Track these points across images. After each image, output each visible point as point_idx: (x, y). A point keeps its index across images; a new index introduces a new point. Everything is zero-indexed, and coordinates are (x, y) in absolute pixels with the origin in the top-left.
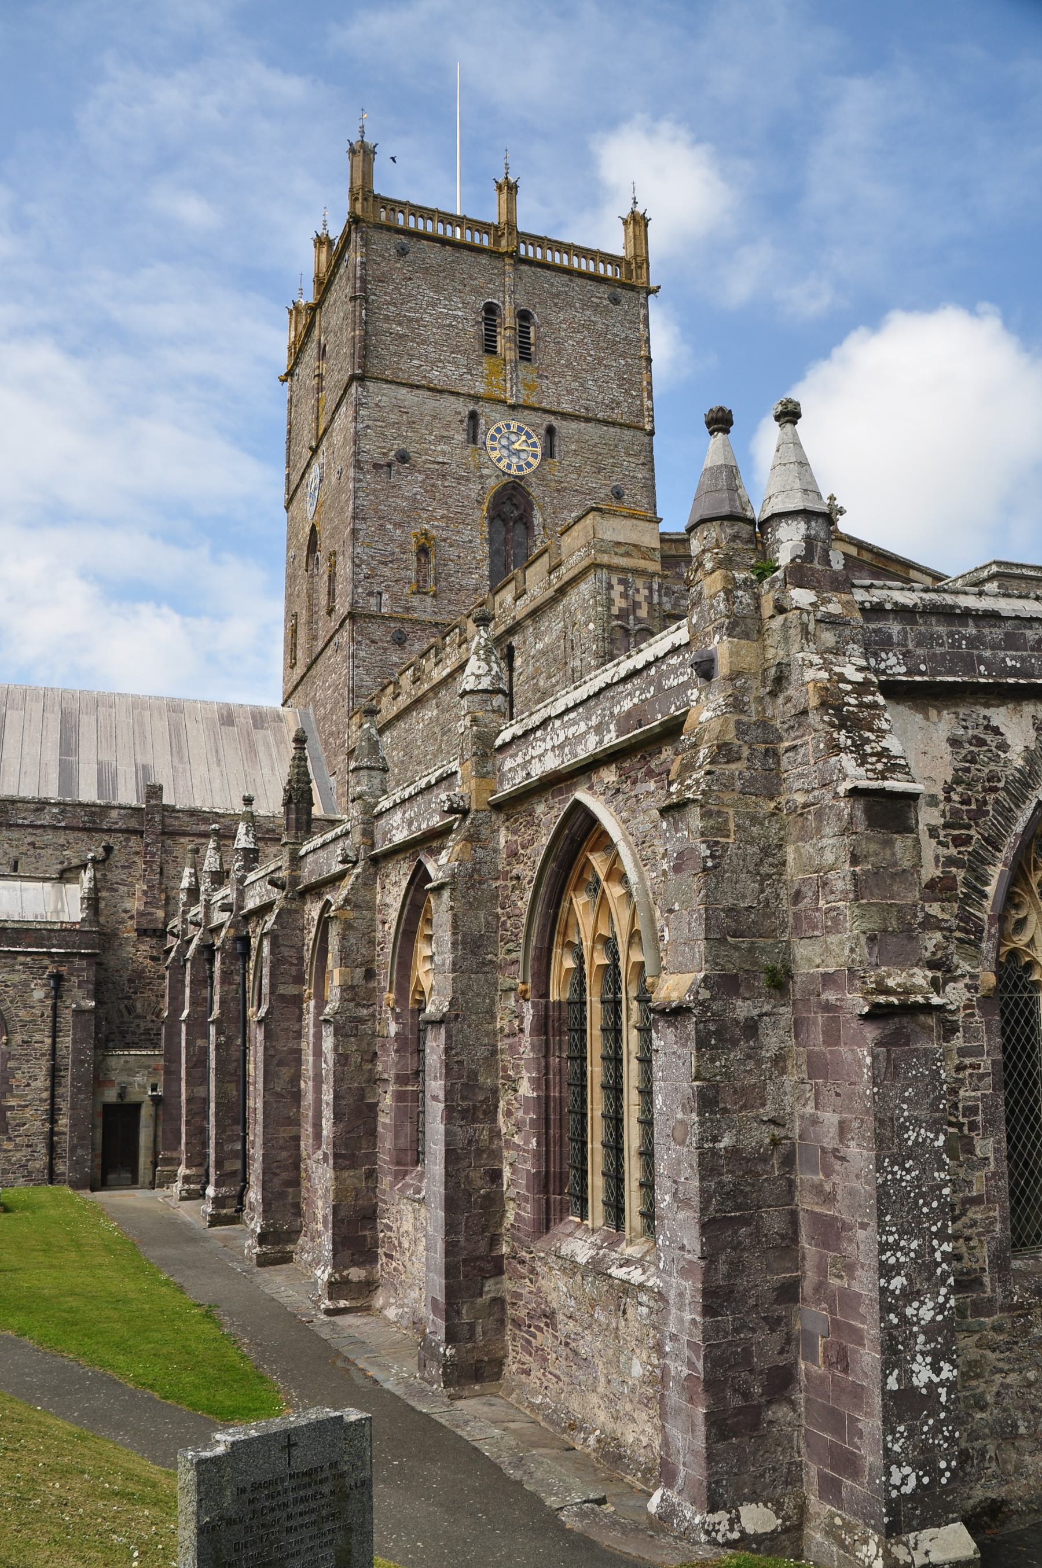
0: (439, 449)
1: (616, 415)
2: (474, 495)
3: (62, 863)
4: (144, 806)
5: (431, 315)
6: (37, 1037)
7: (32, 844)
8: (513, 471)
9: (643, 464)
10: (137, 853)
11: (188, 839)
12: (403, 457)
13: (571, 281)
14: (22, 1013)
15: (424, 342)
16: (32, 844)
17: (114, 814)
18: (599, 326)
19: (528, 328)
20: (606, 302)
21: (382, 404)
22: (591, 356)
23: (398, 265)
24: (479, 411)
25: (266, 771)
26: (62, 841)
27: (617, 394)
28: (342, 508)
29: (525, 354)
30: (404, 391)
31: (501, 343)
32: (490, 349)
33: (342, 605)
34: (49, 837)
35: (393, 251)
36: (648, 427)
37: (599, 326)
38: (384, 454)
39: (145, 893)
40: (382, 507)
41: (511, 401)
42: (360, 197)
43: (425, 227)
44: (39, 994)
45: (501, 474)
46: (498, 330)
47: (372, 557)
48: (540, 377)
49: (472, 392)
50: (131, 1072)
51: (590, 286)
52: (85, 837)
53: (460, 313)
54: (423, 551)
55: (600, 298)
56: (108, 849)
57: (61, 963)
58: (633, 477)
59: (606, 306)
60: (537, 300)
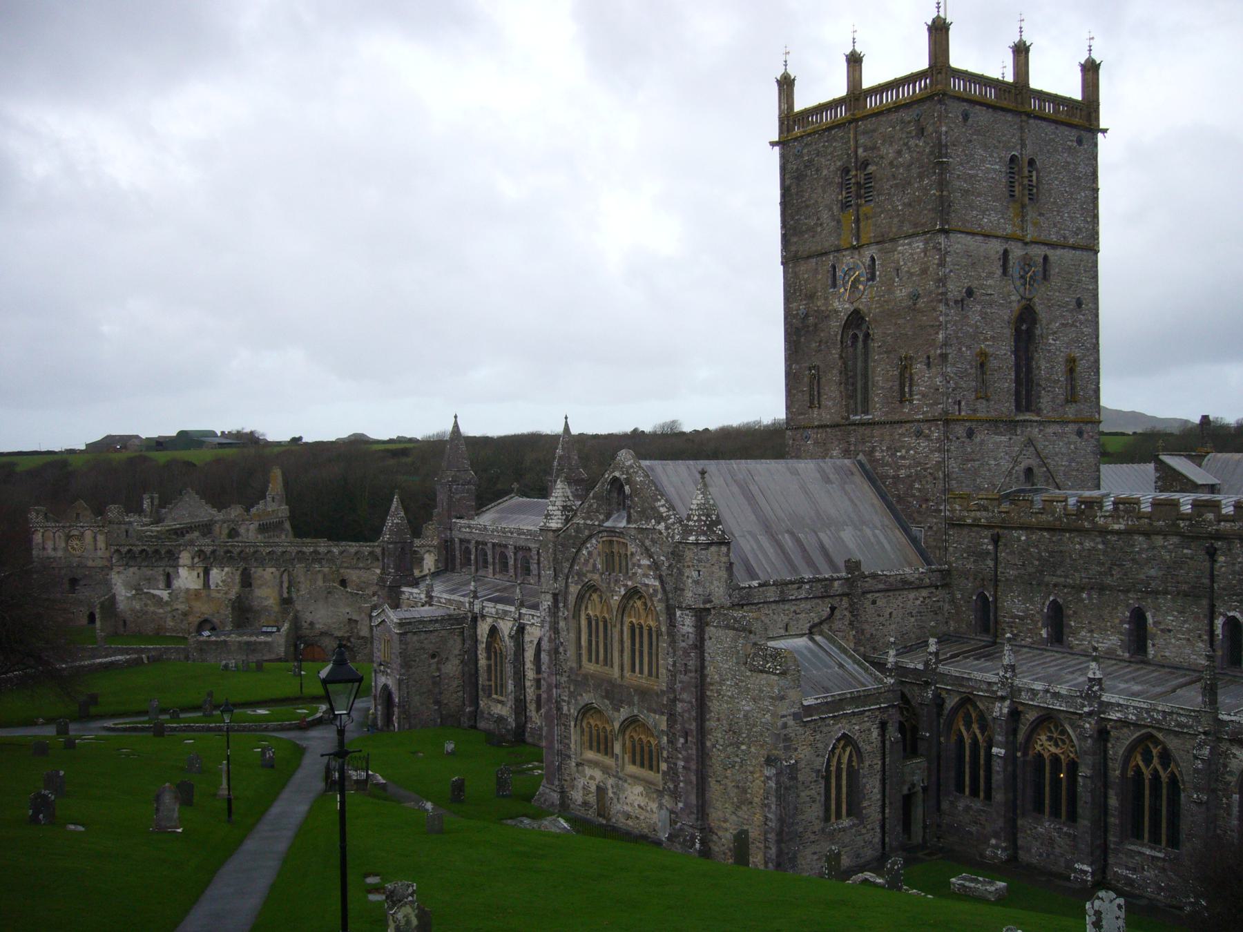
3: (810, 622)
6: (875, 762)
7: (795, 612)
9: (1093, 278)
10: (846, 609)
11: (871, 594)
12: (970, 292)
13: (1056, 128)
14: (868, 747)
15: (979, 195)
16: (795, 612)
17: (836, 584)
20: (1075, 144)
22: (1067, 192)
23: (964, 130)
26: (809, 607)
30: (969, 238)
31: (1017, 189)
34: (803, 605)
38: (959, 291)
39: (854, 636)
40: (960, 335)
41: (1028, 239)
44: (875, 733)
45: (1019, 298)
46: (1017, 177)
48: (1041, 214)
51: (1066, 131)
52: (820, 602)
53: (997, 167)
56: (833, 609)
57: (883, 713)
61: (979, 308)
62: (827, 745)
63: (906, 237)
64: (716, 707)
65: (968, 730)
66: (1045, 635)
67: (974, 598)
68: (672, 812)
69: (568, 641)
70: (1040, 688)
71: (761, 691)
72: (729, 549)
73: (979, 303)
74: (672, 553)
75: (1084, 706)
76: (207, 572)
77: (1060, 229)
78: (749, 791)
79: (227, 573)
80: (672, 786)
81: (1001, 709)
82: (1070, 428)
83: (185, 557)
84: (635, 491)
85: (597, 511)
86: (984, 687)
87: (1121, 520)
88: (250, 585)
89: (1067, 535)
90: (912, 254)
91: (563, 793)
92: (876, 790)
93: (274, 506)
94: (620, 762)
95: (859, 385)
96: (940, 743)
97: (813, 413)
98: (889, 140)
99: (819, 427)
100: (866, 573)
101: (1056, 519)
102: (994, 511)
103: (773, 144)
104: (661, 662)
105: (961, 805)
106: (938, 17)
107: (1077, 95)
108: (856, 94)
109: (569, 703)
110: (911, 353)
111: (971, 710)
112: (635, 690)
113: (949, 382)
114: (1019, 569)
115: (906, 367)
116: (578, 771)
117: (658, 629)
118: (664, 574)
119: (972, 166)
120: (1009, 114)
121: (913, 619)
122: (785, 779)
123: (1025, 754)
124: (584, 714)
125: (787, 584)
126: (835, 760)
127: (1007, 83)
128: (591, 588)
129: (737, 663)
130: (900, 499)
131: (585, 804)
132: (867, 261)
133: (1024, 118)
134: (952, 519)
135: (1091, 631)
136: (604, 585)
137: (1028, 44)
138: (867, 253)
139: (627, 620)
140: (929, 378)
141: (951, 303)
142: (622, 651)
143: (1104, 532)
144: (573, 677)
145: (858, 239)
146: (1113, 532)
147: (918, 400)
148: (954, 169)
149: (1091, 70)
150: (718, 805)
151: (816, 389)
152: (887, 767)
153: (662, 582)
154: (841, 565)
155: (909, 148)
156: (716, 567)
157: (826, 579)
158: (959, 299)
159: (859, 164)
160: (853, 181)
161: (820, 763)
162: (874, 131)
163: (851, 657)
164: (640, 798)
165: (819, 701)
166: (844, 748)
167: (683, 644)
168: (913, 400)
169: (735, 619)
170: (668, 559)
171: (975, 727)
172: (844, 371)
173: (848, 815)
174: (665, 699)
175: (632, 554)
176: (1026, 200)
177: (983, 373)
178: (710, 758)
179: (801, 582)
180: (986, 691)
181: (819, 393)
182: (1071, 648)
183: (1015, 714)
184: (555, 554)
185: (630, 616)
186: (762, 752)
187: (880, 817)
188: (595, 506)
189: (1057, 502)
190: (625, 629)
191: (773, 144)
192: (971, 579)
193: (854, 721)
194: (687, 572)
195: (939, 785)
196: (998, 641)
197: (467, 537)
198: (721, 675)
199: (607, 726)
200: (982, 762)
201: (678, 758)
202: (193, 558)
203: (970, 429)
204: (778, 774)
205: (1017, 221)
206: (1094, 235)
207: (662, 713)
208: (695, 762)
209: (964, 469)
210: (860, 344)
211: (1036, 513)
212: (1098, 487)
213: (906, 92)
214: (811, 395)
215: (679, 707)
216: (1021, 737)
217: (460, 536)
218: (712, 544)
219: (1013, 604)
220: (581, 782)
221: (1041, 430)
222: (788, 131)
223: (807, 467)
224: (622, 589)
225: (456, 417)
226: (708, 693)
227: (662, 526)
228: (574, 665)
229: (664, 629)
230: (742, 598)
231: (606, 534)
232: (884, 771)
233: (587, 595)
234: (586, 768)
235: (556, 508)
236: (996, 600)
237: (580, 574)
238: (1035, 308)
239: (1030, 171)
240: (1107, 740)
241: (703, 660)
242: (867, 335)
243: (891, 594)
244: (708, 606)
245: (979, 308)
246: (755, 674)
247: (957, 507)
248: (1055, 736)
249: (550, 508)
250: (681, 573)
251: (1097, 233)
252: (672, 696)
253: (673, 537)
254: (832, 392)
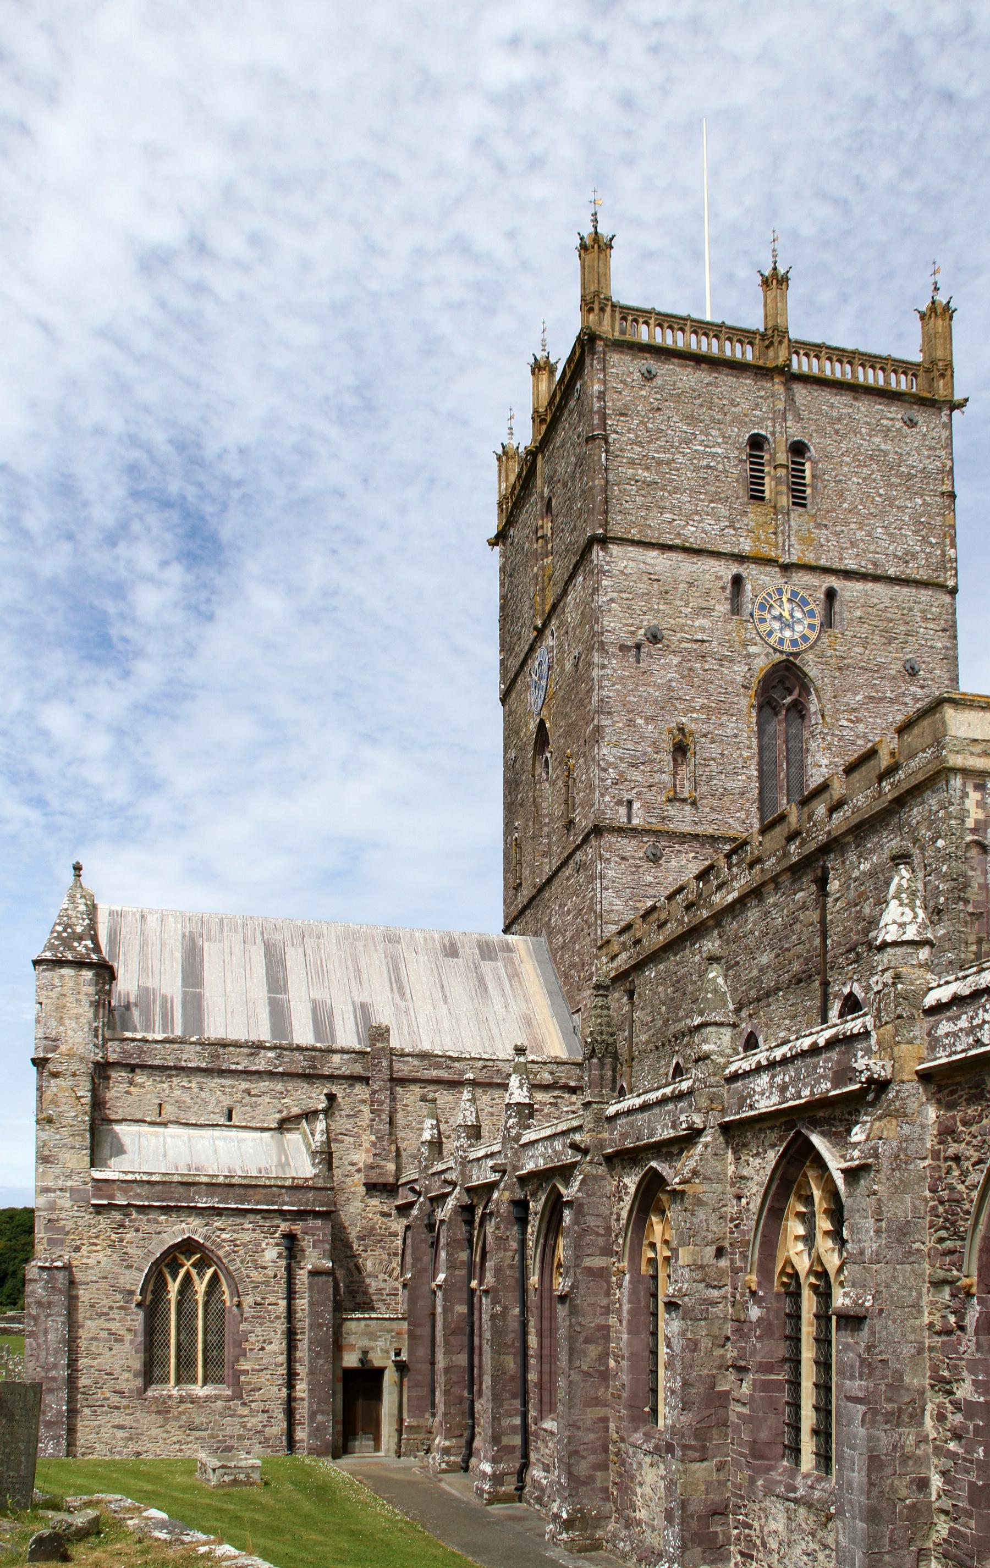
0: (697, 624)
1: (913, 570)
2: (739, 679)
4: (369, 1049)
5: (684, 455)
8: (786, 648)
9: (944, 630)
12: (655, 638)
15: (676, 490)
17: (336, 1058)
18: (891, 457)
19: (803, 464)
20: (899, 424)
21: (628, 571)
22: (880, 495)
24: (745, 575)
25: (499, 1007)
27: (913, 542)
28: (581, 701)
29: (799, 501)
30: (655, 553)
32: (757, 496)
33: (585, 817)
34: (265, 1085)
35: (637, 375)
36: (951, 583)
37: (891, 457)
38: (632, 633)
40: (632, 699)
41: (785, 559)
42: (596, 306)
43: (675, 341)
45: (771, 651)
46: (766, 469)
47: (621, 759)
48: (819, 526)
49: (736, 551)
53: (720, 451)
54: (680, 750)
55: (892, 419)
58: (932, 647)
59: (899, 430)
60: (814, 427)
61: (676, 660)
113: (605, 770)
238: (806, 669)
245: (676, 660)
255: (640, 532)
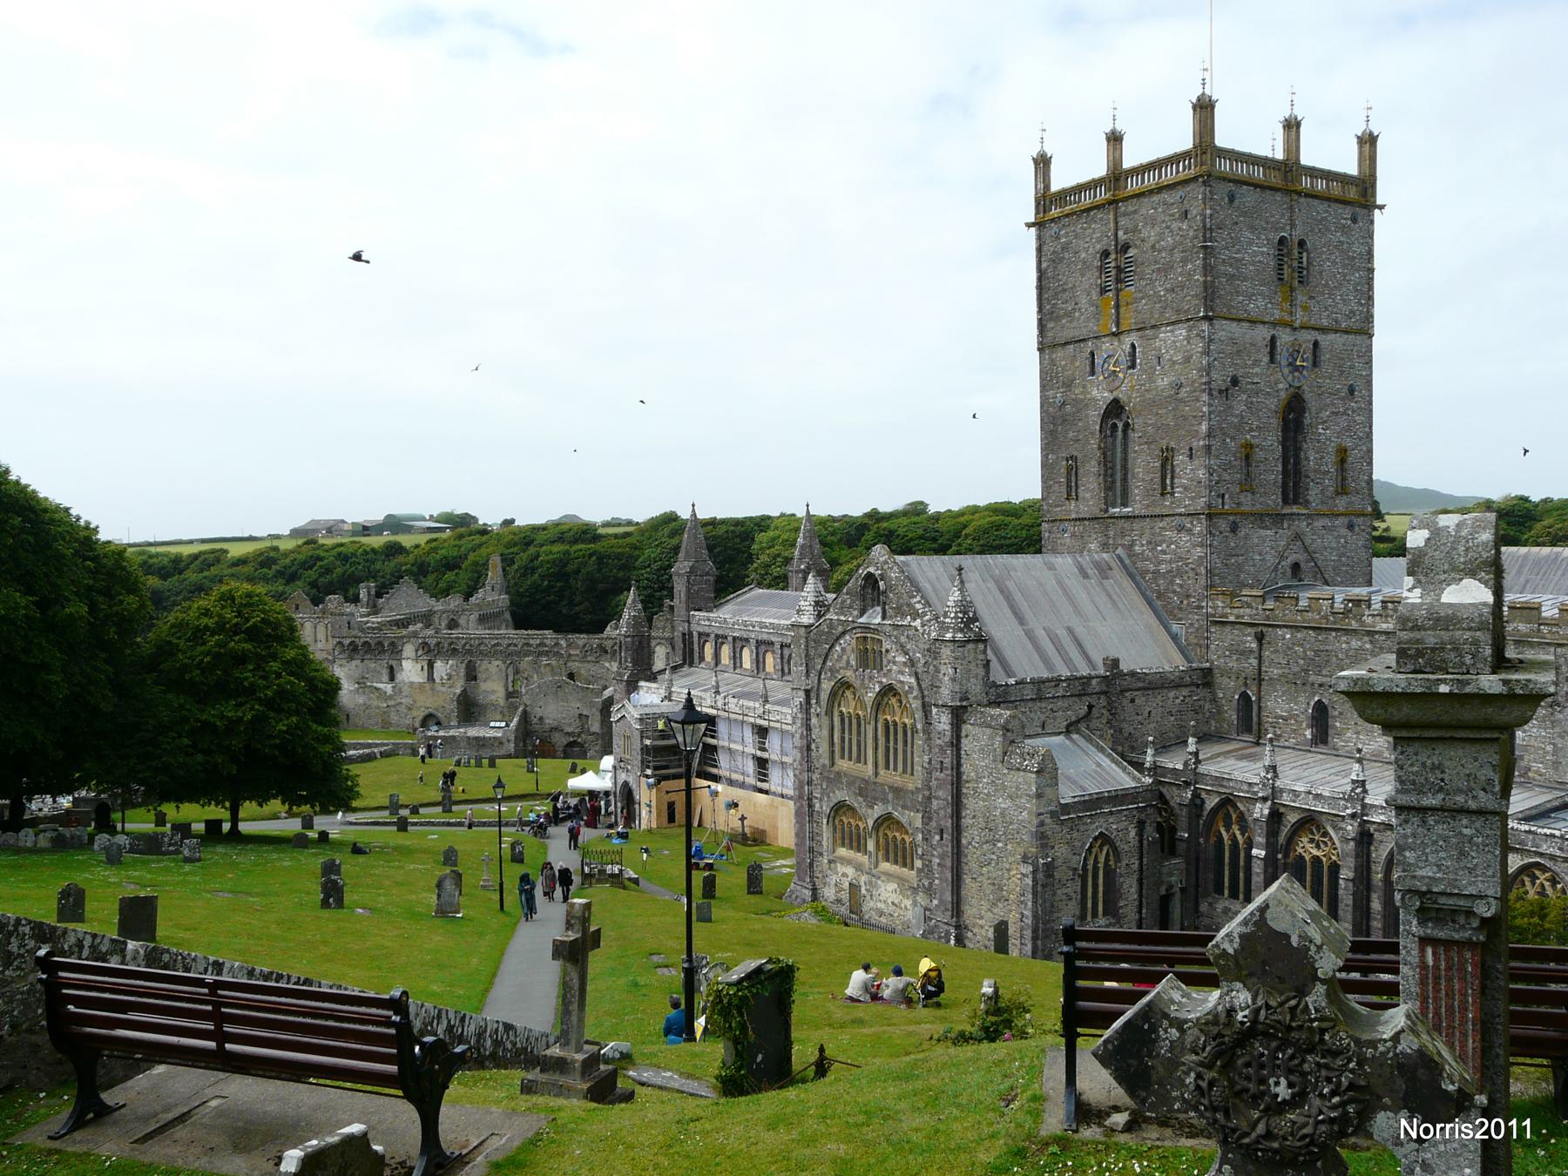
7: (1052, 709)
12: (1235, 381)
13: (1329, 206)
15: (1245, 279)
17: (1094, 682)
20: (1349, 222)
26: (1066, 705)
30: (1234, 324)
31: (1286, 271)
38: (1224, 381)
41: (1297, 324)
44: (1133, 833)
48: (1312, 298)
50: (1171, 875)
51: (1340, 209)
53: (1265, 249)
56: (1090, 707)
61: (1245, 397)
62: (1084, 844)
63: (1168, 324)
64: (971, 805)
65: (1227, 831)
66: (1309, 737)
67: (1237, 697)
68: (926, 909)
69: (820, 738)
70: (1302, 789)
71: (1018, 788)
72: (986, 647)
73: (1244, 393)
74: (929, 650)
75: (1347, 808)
76: (431, 665)
77: (1332, 313)
78: (1005, 888)
79: (452, 666)
80: (926, 884)
81: (1261, 811)
82: (1339, 521)
83: (409, 650)
84: (889, 587)
85: (851, 607)
86: (1245, 787)
87: (1389, 619)
88: (475, 678)
89: (1334, 634)
90: (1174, 342)
91: (814, 890)
92: (1133, 890)
93: (492, 595)
94: (873, 859)
95: (1119, 476)
96: (1199, 844)
97: (1070, 504)
98: (1152, 222)
99: (1076, 520)
100: (1125, 671)
101: (1322, 617)
102: (1257, 609)
103: (1029, 225)
104: (916, 759)
105: (1220, 906)
106: (1203, 94)
107: (1352, 169)
108: (1116, 176)
109: (821, 800)
110: (1173, 444)
111: (1231, 810)
112: (890, 788)
114: (1283, 668)
115: (1167, 459)
116: (830, 868)
117: (914, 726)
118: (919, 671)
119: (1238, 250)
120: (1279, 194)
121: (1172, 718)
122: (1040, 876)
123: (1286, 856)
124: (836, 812)
125: (1042, 682)
126: (1091, 862)
127: (1278, 161)
128: (844, 685)
129: (994, 761)
130: (1160, 595)
131: (839, 901)
132: (1127, 348)
133: (1295, 197)
134: (1214, 616)
135: (1358, 733)
136: (859, 682)
137: (1299, 118)
138: (1128, 340)
139: (881, 718)
140: (1191, 470)
141: (1215, 393)
142: (876, 748)
143: (1369, 633)
144: (826, 774)
145: (1118, 325)
146: (1380, 633)
147: (1179, 492)
148: (1219, 253)
149: (1368, 142)
150: (974, 901)
151: (1073, 479)
152: (1144, 868)
153: (918, 679)
154: (1098, 660)
155: (1171, 231)
156: (972, 666)
157: (1084, 677)
158: (1224, 388)
159: (1119, 247)
160: (1113, 265)
161: (1077, 862)
162: (1135, 212)
163: (1109, 756)
164: (894, 895)
165: (1076, 800)
166: (1101, 847)
167: (939, 742)
168: (1174, 493)
169: (992, 716)
170: (924, 656)
171: (1235, 829)
172: (1107, 462)
173: (1103, 915)
174: (921, 796)
175: (887, 651)
176: (1296, 283)
177: (1248, 465)
178: (966, 856)
179: (1057, 681)
180: (1248, 792)
181: (1076, 483)
182: (1337, 750)
183: (1276, 816)
184: (807, 650)
185: (884, 713)
186: (1018, 849)
187: (1137, 917)
188: (849, 601)
189: (1324, 599)
190: (879, 726)
191: (1029, 225)
192: (1233, 678)
193: (1111, 820)
194: (943, 669)
195: (1197, 886)
196: (1261, 741)
197: (707, 630)
198: (977, 773)
199: (860, 823)
200: (1242, 863)
201: (933, 855)
202: (417, 651)
203: (1234, 522)
204: (1034, 872)
205: (1286, 306)
206: (1369, 318)
207: (918, 811)
208: (950, 859)
209: (1226, 565)
210: (1120, 433)
211: (1302, 611)
212: (1369, 584)
213: (1169, 175)
214: (1069, 486)
215: (935, 802)
216: (1282, 839)
217: (699, 629)
218: (968, 641)
219: (1277, 704)
220: (833, 879)
221: (1309, 524)
222: (1045, 212)
223: (1064, 562)
224: (877, 686)
225: (693, 505)
226: (964, 791)
227: (917, 623)
228: (827, 762)
229: (919, 726)
230: (998, 696)
231: (860, 630)
232: (1141, 870)
233: (841, 692)
234: (839, 865)
235: (807, 603)
236: (1259, 699)
237: (833, 671)
239: (1299, 253)
240: (1370, 843)
241: (959, 757)
242: (1127, 425)
243: (1150, 692)
244: (964, 704)
245: (1245, 397)
246: (1012, 772)
247: (1220, 604)
248: (1316, 838)
249: (802, 603)
250: (937, 670)
251: (1372, 316)
252: (927, 793)
253: (929, 634)
254: (1091, 485)
255: (1228, 310)
